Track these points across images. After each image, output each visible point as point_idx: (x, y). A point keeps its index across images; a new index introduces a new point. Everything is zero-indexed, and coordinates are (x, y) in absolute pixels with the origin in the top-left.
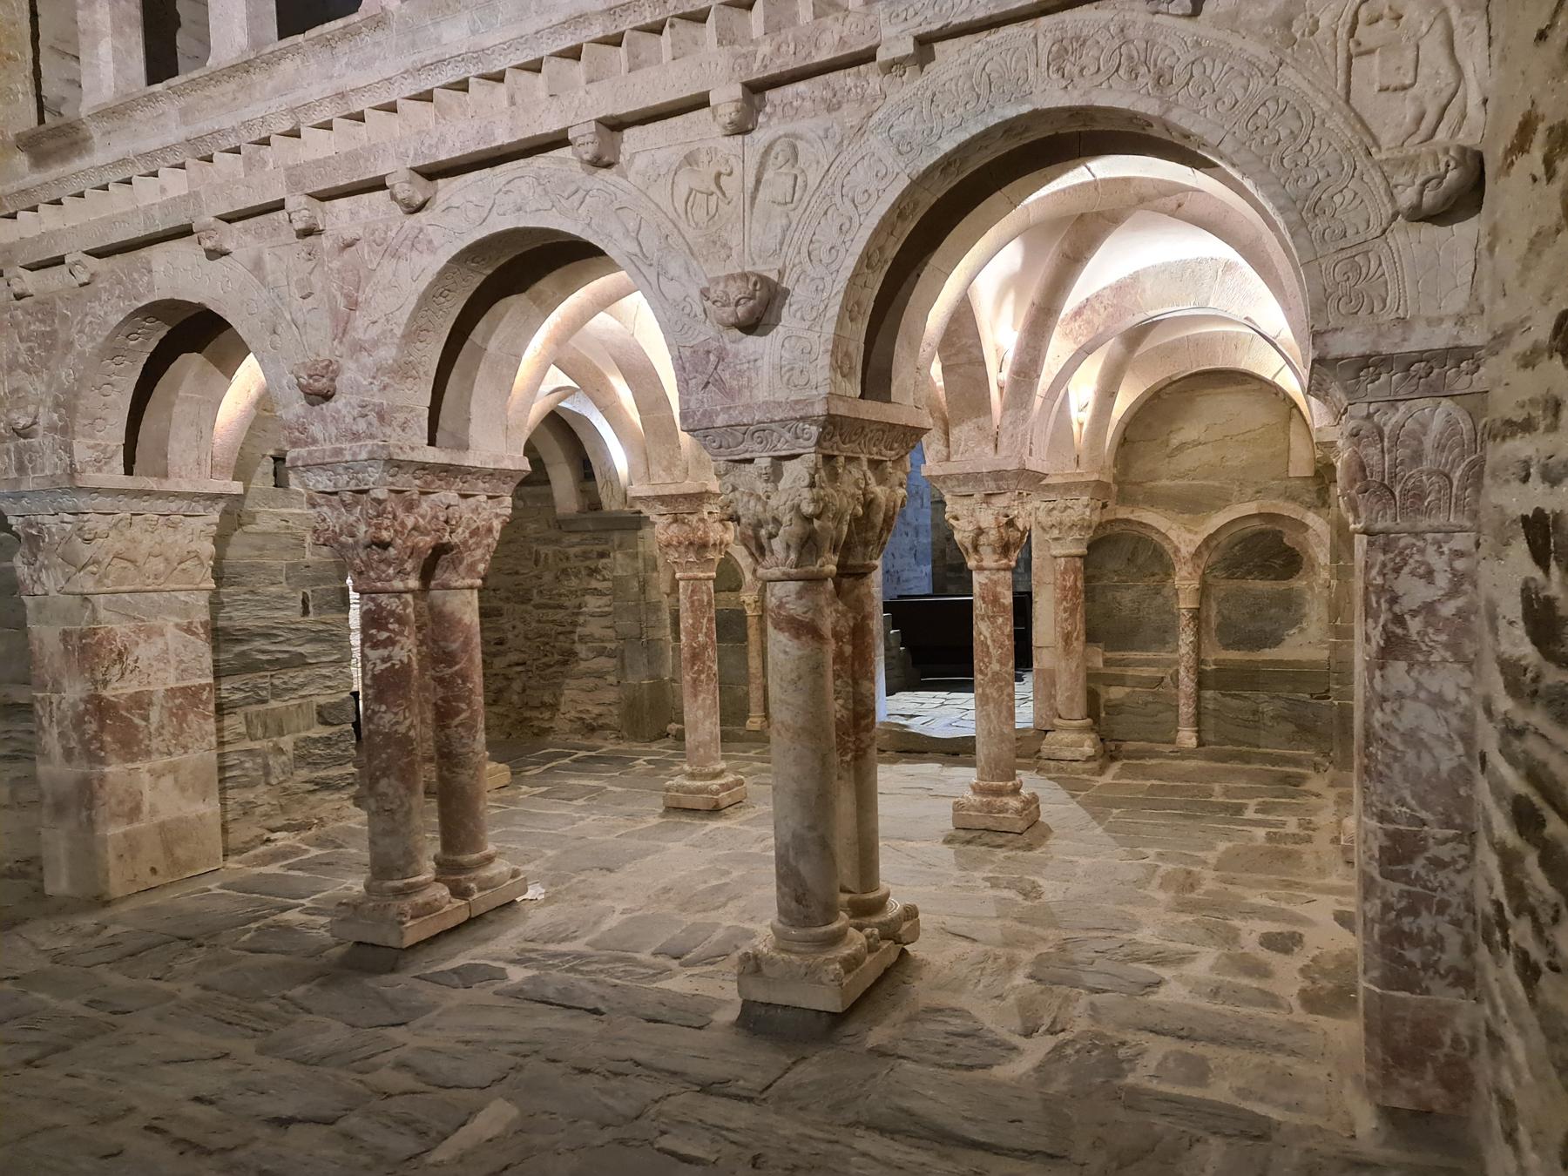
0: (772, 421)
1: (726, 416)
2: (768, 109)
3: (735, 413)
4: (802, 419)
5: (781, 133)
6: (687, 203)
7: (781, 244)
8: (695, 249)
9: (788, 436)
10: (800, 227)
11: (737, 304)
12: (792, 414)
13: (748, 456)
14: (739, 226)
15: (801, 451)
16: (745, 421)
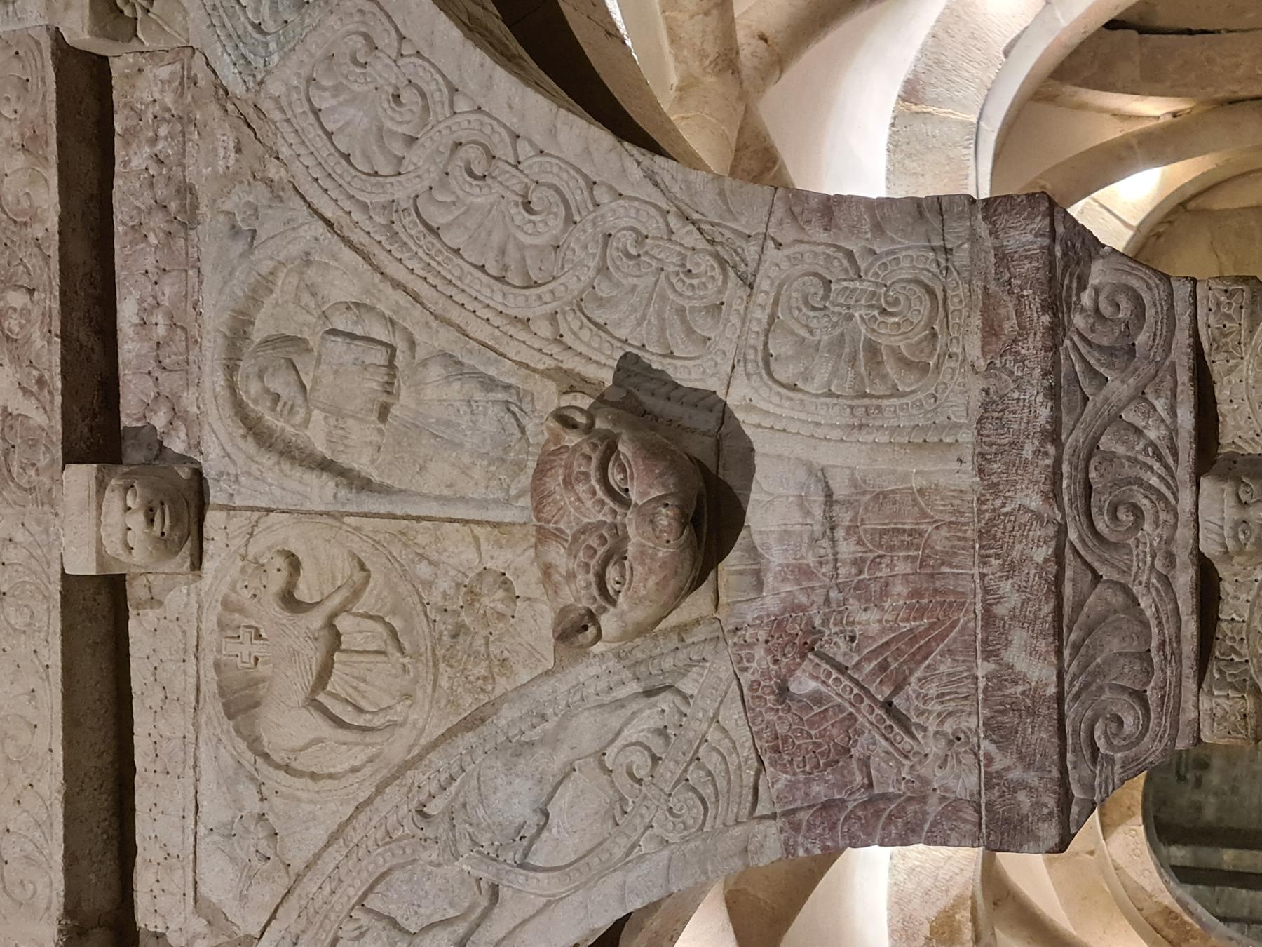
0: (1054, 435)
1: (1019, 636)
2: (159, 420)
3: (1010, 598)
4: (1056, 304)
5: (220, 380)
6: (339, 723)
7: (490, 384)
8: (468, 704)
9: (1119, 387)
10: (455, 315)
11: (620, 498)
12: (1032, 346)
13: (1185, 579)
14: (422, 535)
15: (1182, 338)
16: (1042, 553)
